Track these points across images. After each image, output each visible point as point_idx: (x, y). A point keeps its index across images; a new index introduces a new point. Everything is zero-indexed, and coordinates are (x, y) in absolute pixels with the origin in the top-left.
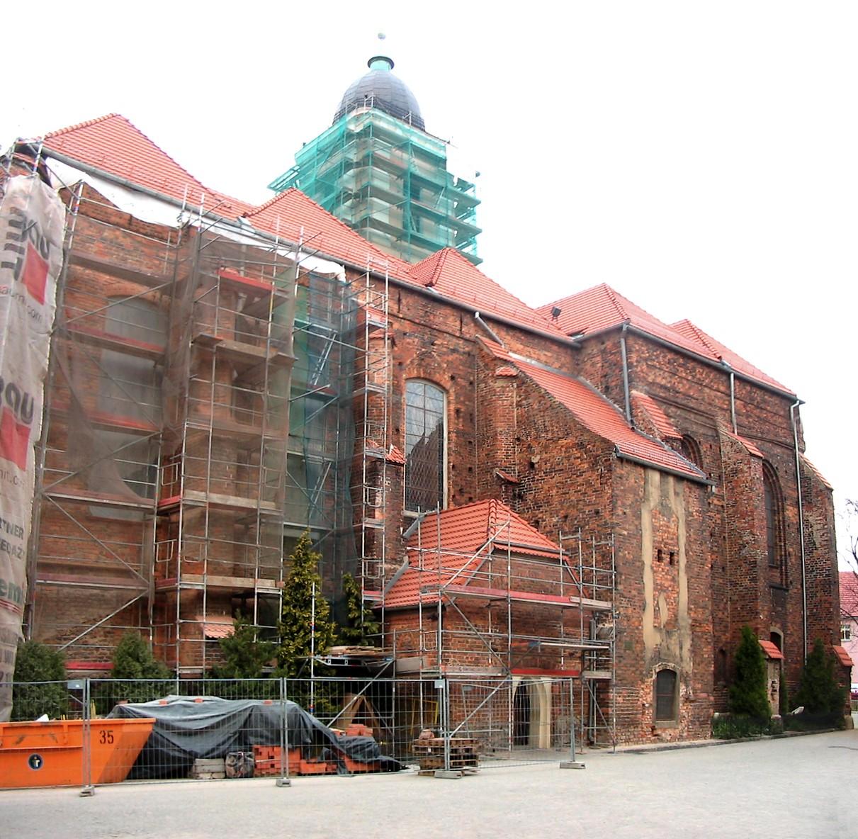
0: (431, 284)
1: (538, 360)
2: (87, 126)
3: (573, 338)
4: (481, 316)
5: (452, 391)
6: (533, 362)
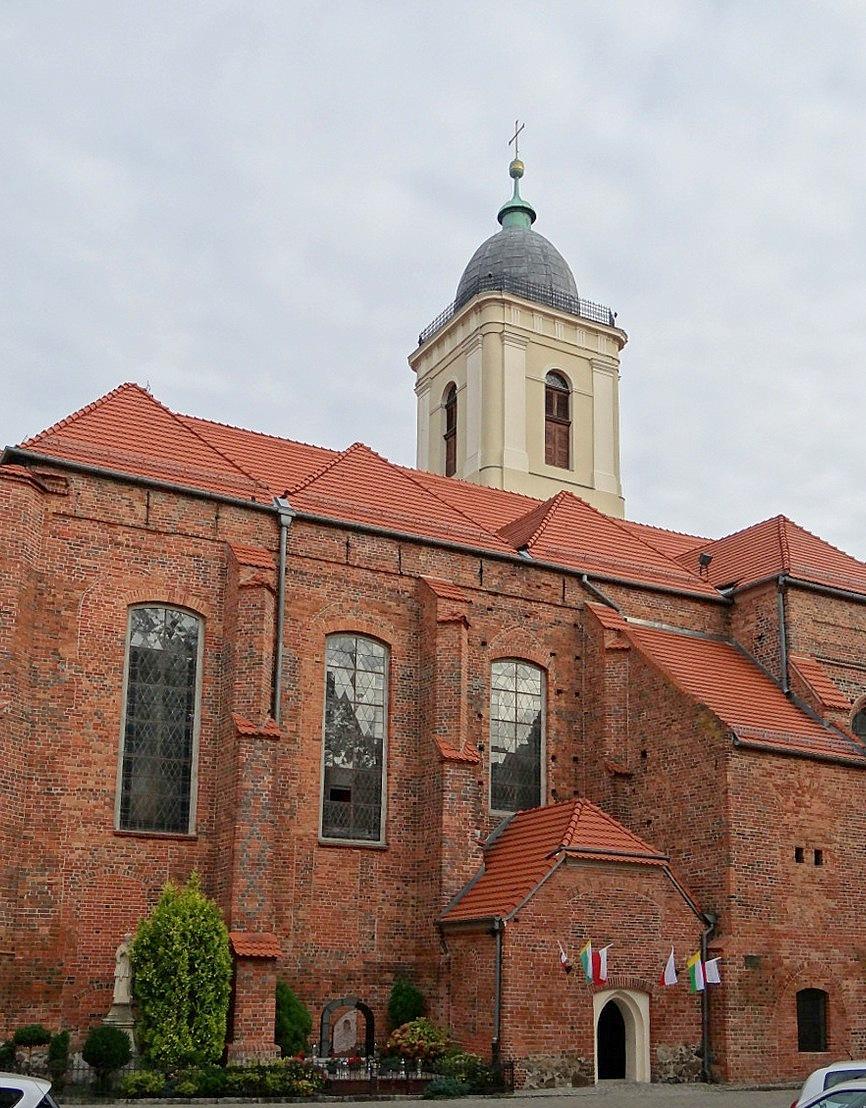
0: (525, 547)
1: (671, 624)
3: (723, 592)
4: (589, 578)
6: (664, 626)
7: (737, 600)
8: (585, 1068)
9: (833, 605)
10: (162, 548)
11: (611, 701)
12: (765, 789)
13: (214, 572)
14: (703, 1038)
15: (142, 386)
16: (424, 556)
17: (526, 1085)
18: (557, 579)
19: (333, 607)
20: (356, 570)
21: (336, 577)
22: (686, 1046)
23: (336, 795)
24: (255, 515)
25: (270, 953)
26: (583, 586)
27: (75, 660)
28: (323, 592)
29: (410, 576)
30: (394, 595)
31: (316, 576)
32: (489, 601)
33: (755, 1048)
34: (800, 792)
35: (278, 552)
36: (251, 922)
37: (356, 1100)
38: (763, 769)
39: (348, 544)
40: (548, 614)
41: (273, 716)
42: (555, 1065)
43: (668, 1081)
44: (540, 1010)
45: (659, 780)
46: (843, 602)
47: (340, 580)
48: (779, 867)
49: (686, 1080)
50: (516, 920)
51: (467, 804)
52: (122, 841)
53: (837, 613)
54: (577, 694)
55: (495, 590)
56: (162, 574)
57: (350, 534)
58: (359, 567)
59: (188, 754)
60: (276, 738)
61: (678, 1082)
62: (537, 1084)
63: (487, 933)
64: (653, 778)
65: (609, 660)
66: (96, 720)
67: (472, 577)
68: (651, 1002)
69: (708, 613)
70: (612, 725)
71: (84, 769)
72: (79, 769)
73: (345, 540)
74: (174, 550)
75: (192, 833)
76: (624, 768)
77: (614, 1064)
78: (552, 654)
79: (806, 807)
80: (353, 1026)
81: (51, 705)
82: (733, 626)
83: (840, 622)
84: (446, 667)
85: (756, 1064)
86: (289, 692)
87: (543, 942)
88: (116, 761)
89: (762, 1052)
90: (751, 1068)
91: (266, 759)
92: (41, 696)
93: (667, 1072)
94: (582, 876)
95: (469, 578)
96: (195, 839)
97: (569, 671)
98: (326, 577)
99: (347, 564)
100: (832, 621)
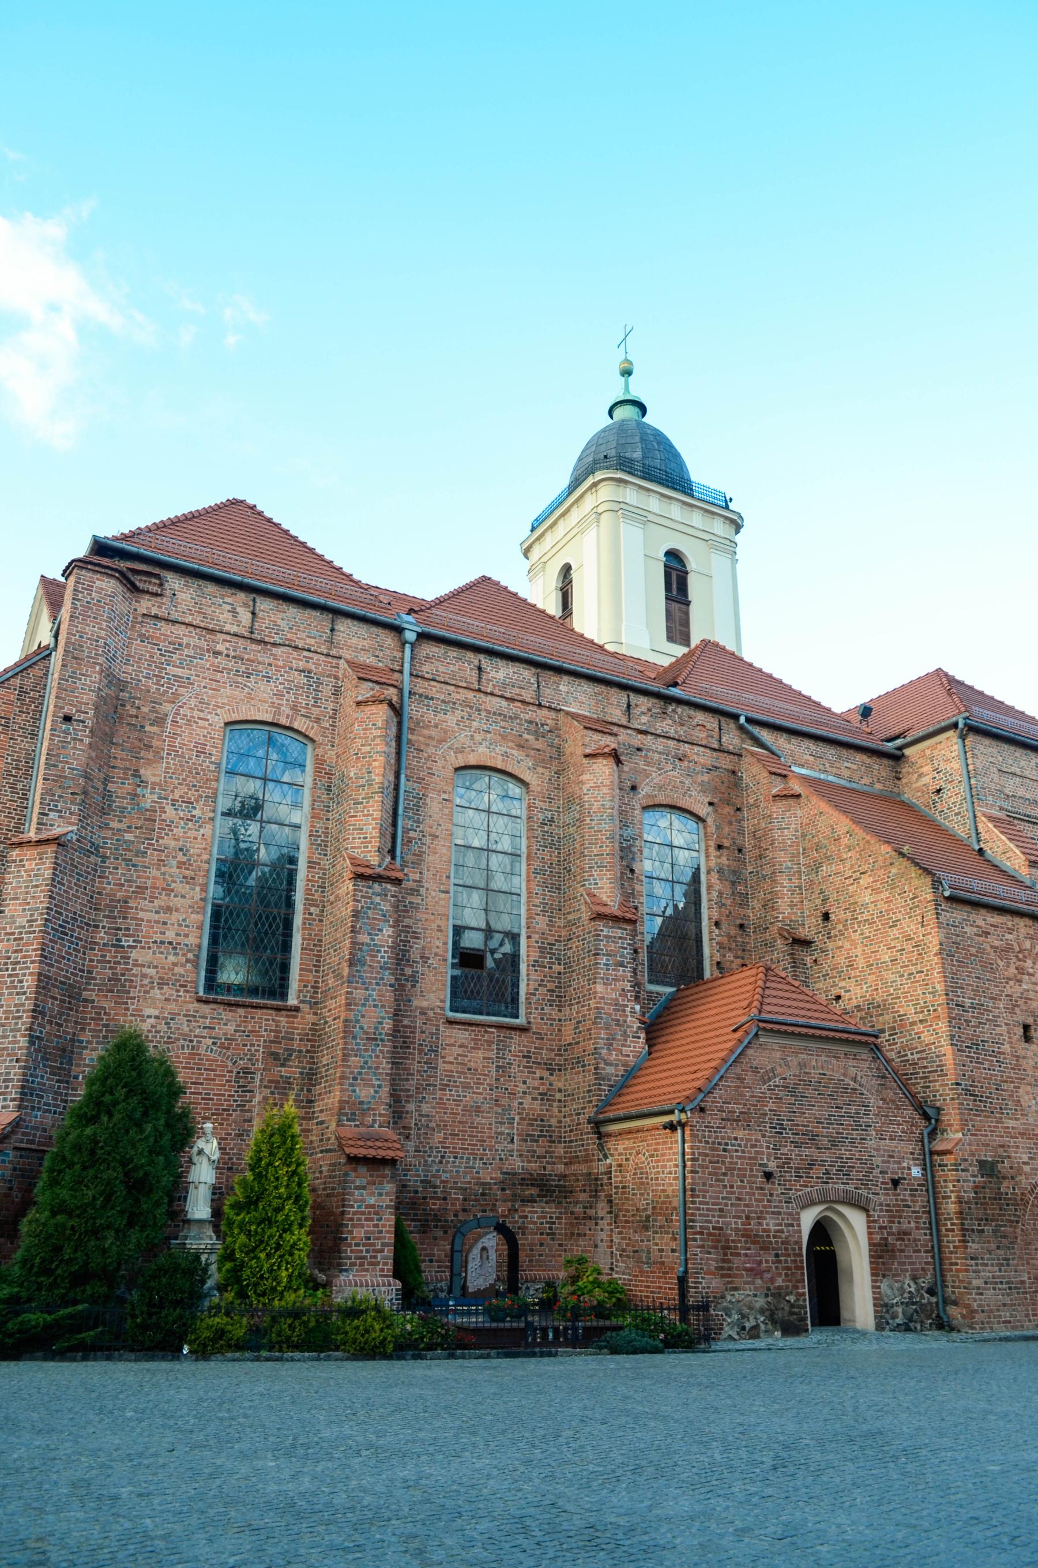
0: (675, 684)
1: (837, 775)
2: (194, 517)
3: (890, 744)
5: (710, 821)
7: (907, 752)
8: (797, 1310)
9: (1017, 754)
10: (267, 661)
11: (783, 858)
12: (981, 951)
13: (327, 690)
14: (934, 1269)
15: (250, 501)
16: (565, 685)
17: (725, 1335)
18: (712, 720)
19: (463, 738)
20: (489, 698)
21: (466, 703)
22: (914, 1279)
23: (468, 959)
24: (374, 630)
25: (390, 1154)
26: (741, 728)
27: (159, 785)
28: (451, 720)
29: (549, 708)
30: (532, 727)
31: (443, 701)
32: (638, 740)
33: (1001, 1283)
34: (1021, 956)
35: (401, 672)
36: (364, 1113)
37: (508, 1355)
38: (977, 926)
39: (480, 669)
40: (703, 757)
41: (393, 858)
42: (758, 1305)
43: (898, 1328)
44: (737, 1230)
45: (847, 945)
46: (1029, 752)
47: (471, 708)
48: (1006, 1048)
49: (919, 1327)
50: (702, 1110)
51: (624, 971)
52: (206, 1009)
53: (1023, 763)
54: (740, 851)
55: (644, 728)
56: (265, 690)
57: (482, 657)
58: (492, 694)
59: (290, 904)
60: (397, 882)
61: (908, 1329)
62: (738, 1334)
63: (665, 1128)
64: (840, 943)
65: (778, 808)
66: (180, 857)
67: (618, 712)
68: (868, 1222)
69: (876, 767)
70: (785, 883)
71: (162, 917)
72: (156, 917)
73: (476, 662)
74: (281, 663)
75: (292, 1001)
76: (803, 933)
77: (828, 1309)
78: (711, 804)
79: (1029, 974)
80: (493, 1255)
81: (128, 837)
82: (904, 781)
83: (1027, 773)
84: (595, 808)
85: (1004, 1305)
86: (412, 834)
87: (736, 1139)
88: (204, 908)
89: (1010, 1288)
90: (998, 1310)
91: (386, 907)
92: (114, 825)
93: (894, 1317)
94: (778, 1055)
95: (616, 714)
96: (297, 1009)
97: (730, 823)
98: (454, 703)
99: (479, 690)
100: (1018, 771)
